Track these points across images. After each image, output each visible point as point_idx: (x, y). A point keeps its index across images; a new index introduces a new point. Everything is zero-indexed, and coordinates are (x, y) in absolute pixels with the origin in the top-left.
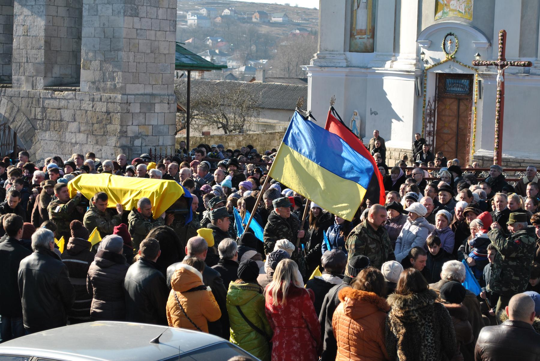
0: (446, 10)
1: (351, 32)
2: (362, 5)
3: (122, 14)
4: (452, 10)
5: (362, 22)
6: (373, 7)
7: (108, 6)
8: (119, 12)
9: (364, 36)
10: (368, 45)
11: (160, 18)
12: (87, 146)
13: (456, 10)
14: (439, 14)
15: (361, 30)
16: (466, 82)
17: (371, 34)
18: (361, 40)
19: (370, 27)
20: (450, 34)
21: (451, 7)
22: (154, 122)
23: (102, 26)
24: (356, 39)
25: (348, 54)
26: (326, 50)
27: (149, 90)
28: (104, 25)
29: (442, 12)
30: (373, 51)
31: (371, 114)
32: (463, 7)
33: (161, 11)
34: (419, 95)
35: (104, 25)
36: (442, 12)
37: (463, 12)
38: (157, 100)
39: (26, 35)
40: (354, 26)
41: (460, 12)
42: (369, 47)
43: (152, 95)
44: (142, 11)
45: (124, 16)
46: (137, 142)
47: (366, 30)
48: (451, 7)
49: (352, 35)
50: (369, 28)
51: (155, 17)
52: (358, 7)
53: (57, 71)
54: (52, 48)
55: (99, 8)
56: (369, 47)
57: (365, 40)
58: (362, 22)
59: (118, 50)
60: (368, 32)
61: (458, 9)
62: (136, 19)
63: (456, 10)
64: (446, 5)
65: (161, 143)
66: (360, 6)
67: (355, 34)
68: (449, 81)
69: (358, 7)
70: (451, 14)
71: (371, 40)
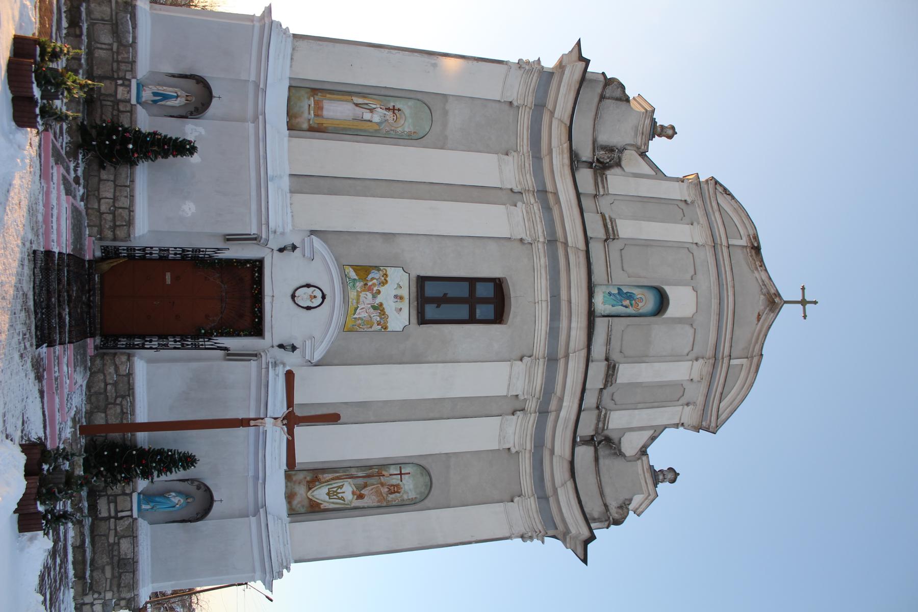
0: (359, 285)
1: (319, 91)
2: (359, 111)
4: (358, 296)
6: (357, 130)
9: (312, 112)
10: (298, 120)
13: (358, 303)
14: (353, 275)
15: (321, 108)
17: (316, 126)
18: (307, 107)
19: (326, 123)
20: (324, 297)
21: (362, 295)
24: (309, 99)
26: (293, 49)
29: (356, 277)
30: (290, 127)
34: (228, 240)
36: (356, 277)
37: (355, 316)
40: (328, 96)
41: (356, 309)
42: (295, 121)
47: (321, 116)
49: (314, 91)
50: (324, 122)
52: (357, 105)
56: (295, 121)
57: (306, 115)
58: (337, 111)
60: (319, 120)
61: (361, 306)
63: (358, 303)
64: (366, 284)
66: (357, 108)
67: (317, 98)
69: (357, 105)
71: (305, 126)
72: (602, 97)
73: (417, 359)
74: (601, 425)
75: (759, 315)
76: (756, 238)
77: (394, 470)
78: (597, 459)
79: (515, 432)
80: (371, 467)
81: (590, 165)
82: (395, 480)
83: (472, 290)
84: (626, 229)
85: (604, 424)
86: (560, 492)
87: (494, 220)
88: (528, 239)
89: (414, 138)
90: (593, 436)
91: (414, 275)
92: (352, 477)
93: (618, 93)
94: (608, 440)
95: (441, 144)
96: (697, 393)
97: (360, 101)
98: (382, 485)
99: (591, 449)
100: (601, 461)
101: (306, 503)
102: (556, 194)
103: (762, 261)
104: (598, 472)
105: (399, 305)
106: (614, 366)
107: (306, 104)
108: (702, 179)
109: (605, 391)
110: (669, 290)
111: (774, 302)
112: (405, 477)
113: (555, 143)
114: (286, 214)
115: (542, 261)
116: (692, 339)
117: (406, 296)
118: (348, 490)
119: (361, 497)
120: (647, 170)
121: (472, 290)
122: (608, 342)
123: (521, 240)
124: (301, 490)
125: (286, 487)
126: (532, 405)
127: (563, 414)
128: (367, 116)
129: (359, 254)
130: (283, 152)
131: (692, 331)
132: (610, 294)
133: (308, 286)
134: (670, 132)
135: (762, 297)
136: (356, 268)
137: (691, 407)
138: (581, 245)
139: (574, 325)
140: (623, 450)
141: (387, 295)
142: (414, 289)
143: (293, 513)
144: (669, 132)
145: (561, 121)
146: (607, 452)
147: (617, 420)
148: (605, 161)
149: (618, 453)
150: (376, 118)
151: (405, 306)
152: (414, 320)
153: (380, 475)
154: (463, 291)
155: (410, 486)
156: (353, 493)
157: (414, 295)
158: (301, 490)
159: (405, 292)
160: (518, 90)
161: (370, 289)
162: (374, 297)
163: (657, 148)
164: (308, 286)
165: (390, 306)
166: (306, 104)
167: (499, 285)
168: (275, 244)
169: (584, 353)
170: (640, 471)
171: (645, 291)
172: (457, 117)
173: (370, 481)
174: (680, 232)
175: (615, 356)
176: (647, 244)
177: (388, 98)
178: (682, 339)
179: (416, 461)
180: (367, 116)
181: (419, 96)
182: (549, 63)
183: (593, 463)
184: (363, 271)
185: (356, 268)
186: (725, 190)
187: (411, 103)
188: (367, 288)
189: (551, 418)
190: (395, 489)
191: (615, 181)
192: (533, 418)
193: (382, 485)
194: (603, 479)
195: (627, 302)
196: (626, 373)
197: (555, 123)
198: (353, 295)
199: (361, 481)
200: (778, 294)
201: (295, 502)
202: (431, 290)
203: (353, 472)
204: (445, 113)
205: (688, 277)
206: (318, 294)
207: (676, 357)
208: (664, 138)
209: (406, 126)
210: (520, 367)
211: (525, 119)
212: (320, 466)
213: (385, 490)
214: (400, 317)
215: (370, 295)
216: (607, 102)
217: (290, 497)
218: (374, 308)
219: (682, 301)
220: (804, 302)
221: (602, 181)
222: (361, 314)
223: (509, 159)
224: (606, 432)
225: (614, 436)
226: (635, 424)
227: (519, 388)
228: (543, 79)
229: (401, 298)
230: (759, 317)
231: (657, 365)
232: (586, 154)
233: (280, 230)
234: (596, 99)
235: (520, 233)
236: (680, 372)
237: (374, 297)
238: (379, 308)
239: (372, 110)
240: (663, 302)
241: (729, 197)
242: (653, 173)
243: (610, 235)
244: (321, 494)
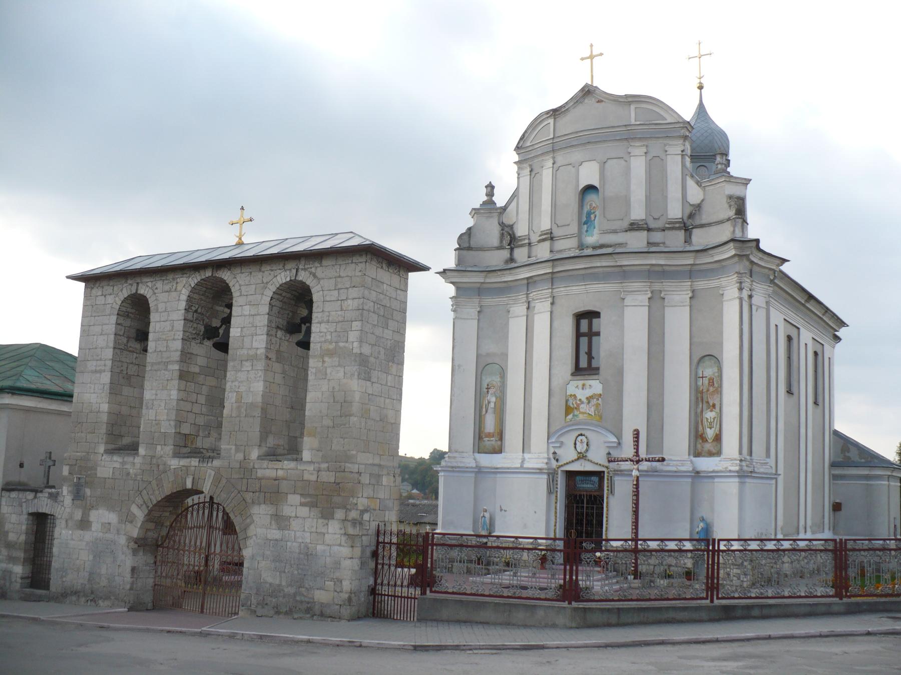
0: (576, 413)
1: (480, 435)
2: (490, 411)
3: (356, 377)
5: (490, 424)
7: (339, 368)
8: (353, 375)
11: (389, 384)
12: (310, 520)
14: (570, 416)
15: (489, 433)
16: (595, 479)
20: (581, 435)
21: (581, 410)
22: (381, 496)
23: (331, 390)
25: (477, 455)
27: (377, 461)
28: (333, 388)
30: (500, 451)
31: (501, 510)
32: (593, 409)
33: (389, 377)
35: (333, 388)
38: (385, 472)
39: (239, 400)
43: (380, 466)
44: (375, 374)
45: (359, 378)
46: (366, 517)
48: (581, 410)
49: (480, 438)
51: (384, 383)
53: (271, 441)
54: (268, 416)
55: (329, 371)
57: (493, 443)
59: (350, 415)
62: (369, 383)
65: (386, 519)
68: (578, 478)
70: (581, 417)
71: (499, 443)
72: (469, 248)
73: (620, 372)
74: (677, 225)
75: (598, 102)
76: (547, 112)
77: (700, 383)
78: (702, 226)
79: (678, 296)
80: (697, 398)
81: (512, 249)
82: (706, 381)
83: (584, 335)
84: (545, 224)
85: (677, 223)
86: (717, 258)
87: (542, 322)
88: (550, 300)
89: (503, 374)
90: (686, 230)
91: (570, 377)
92: (702, 411)
93: (466, 237)
94: (691, 216)
95: (505, 356)
96: (656, 148)
97: (484, 410)
98: (708, 390)
99: (696, 233)
100: (704, 222)
101: (715, 443)
102: (528, 278)
103: (561, 107)
104: (709, 225)
105: (587, 386)
106: (632, 224)
107: (489, 442)
108: (516, 158)
109: (652, 226)
110: (581, 187)
111: (588, 92)
112: (706, 374)
113: (499, 280)
114: (537, 458)
115: (561, 290)
116: (615, 160)
117: (582, 382)
118: (710, 415)
119: (714, 406)
120: (514, 204)
121: (584, 335)
122: (615, 232)
123: (552, 304)
124: (708, 446)
125: (704, 456)
126: (657, 286)
127: (662, 262)
128: (492, 405)
129: (559, 411)
130: (510, 458)
132: (587, 231)
133: (575, 444)
134: (489, 189)
135: (586, 101)
136: (567, 414)
137: (667, 148)
138: (550, 264)
139: (599, 264)
140: (699, 202)
141: (582, 395)
142: (578, 377)
143: (719, 453)
144: (490, 188)
145: (486, 277)
146: (697, 217)
147: (675, 211)
148: (510, 239)
149: (699, 207)
150: (493, 399)
151: (588, 383)
152: (596, 377)
153: (702, 392)
154: (584, 341)
155: (709, 371)
156: (711, 411)
157: (582, 377)
158: (708, 446)
159: (580, 383)
160: (471, 310)
161: (578, 405)
162: (582, 403)
163: (500, 199)
164: (575, 444)
165: (588, 392)
166: (489, 442)
167: (580, 317)
168: (554, 464)
169: (614, 256)
170: (712, 188)
171: (585, 203)
172: (490, 347)
173: (705, 400)
174: (547, 175)
175: (626, 224)
176: (554, 205)
177: (481, 393)
178: (614, 167)
179: (694, 367)
180: (492, 405)
181: (479, 373)
182: (451, 290)
183: (704, 229)
184: (568, 410)
185: (567, 414)
186: (521, 139)
187: (484, 378)
188: (577, 408)
189: (667, 268)
190: (711, 382)
191: (521, 230)
193: (708, 390)
194: (715, 220)
195: (592, 216)
196: (638, 213)
197: (488, 280)
198: (581, 417)
199: (705, 405)
200: (582, 89)
201: (714, 451)
202: (583, 363)
203: (699, 410)
204: (488, 355)
205: (573, 170)
206: (580, 437)
207: (627, 172)
208: (495, 191)
209: (496, 379)
210: (629, 300)
211: (489, 301)
212: (693, 434)
213: (711, 389)
214: (595, 386)
215: (582, 406)
216: (473, 244)
217: (711, 454)
218: (589, 403)
219: (589, 174)
220: (591, 57)
221: (521, 240)
222: (592, 411)
223: (511, 309)
224: (685, 218)
225: (688, 210)
226: (679, 195)
227: (644, 298)
228: (463, 293)
229: (584, 385)
230: (599, 101)
231: (633, 187)
232: (505, 254)
233: (546, 461)
234: (471, 252)
235: (548, 304)
236: (638, 165)
237: (582, 403)
238: (589, 399)
239: (489, 402)
240: (590, 188)
241: (526, 135)
242: (515, 200)
243: (550, 237)
244: (710, 433)
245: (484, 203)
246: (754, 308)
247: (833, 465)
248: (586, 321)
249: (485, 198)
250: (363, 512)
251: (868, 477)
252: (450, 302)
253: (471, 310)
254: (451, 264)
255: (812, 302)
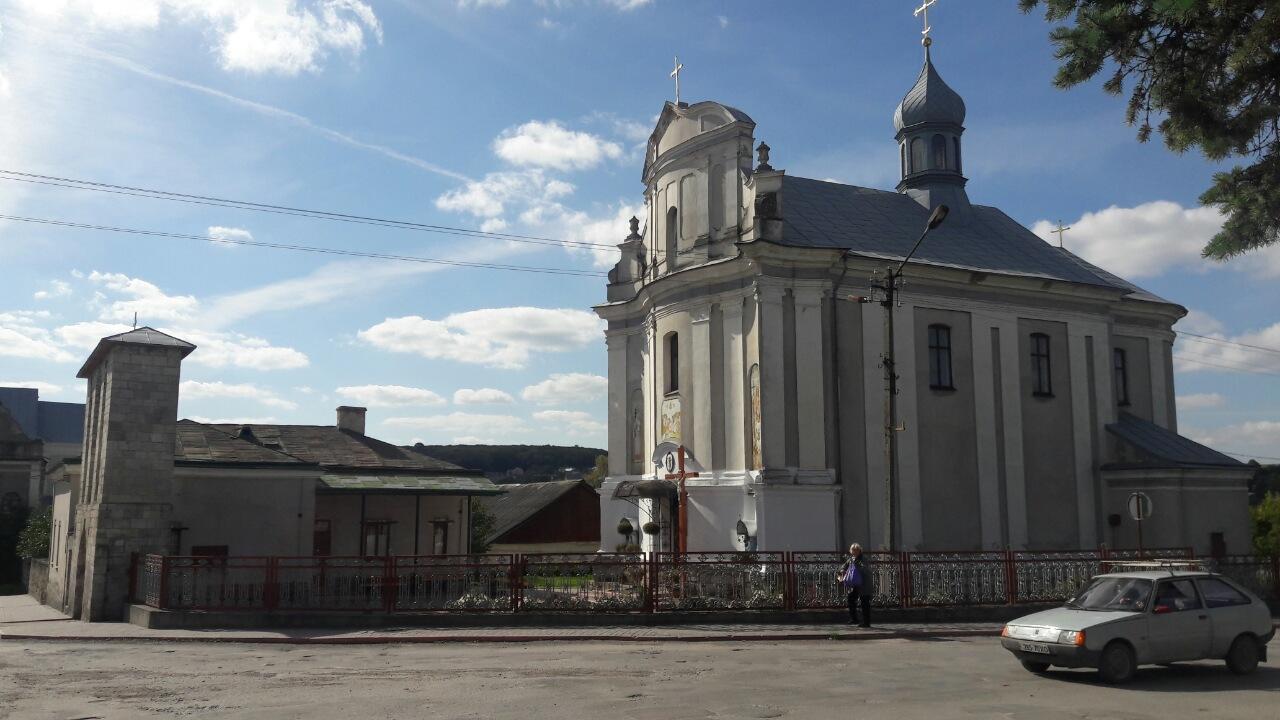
126: (715, 299)
131: (687, 180)
169: (679, 276)
189: (725, 280)
192: (725, 295)
216: (620, 280)
228: (614, 326)
240: (673, 211)
245: (629, 238)
246: (798, 309)
247: (1098, 468)
248: (672, 340)
249: (630, 232)
250: (113, 540)
251: (1147, 482)
252: (605, 336)
253: (622, 341)
254: (603, 301)
255: (989, 278)
